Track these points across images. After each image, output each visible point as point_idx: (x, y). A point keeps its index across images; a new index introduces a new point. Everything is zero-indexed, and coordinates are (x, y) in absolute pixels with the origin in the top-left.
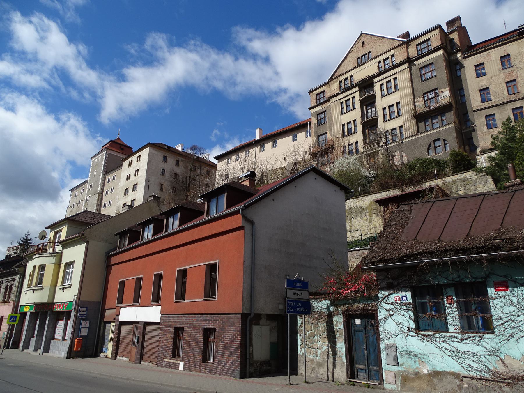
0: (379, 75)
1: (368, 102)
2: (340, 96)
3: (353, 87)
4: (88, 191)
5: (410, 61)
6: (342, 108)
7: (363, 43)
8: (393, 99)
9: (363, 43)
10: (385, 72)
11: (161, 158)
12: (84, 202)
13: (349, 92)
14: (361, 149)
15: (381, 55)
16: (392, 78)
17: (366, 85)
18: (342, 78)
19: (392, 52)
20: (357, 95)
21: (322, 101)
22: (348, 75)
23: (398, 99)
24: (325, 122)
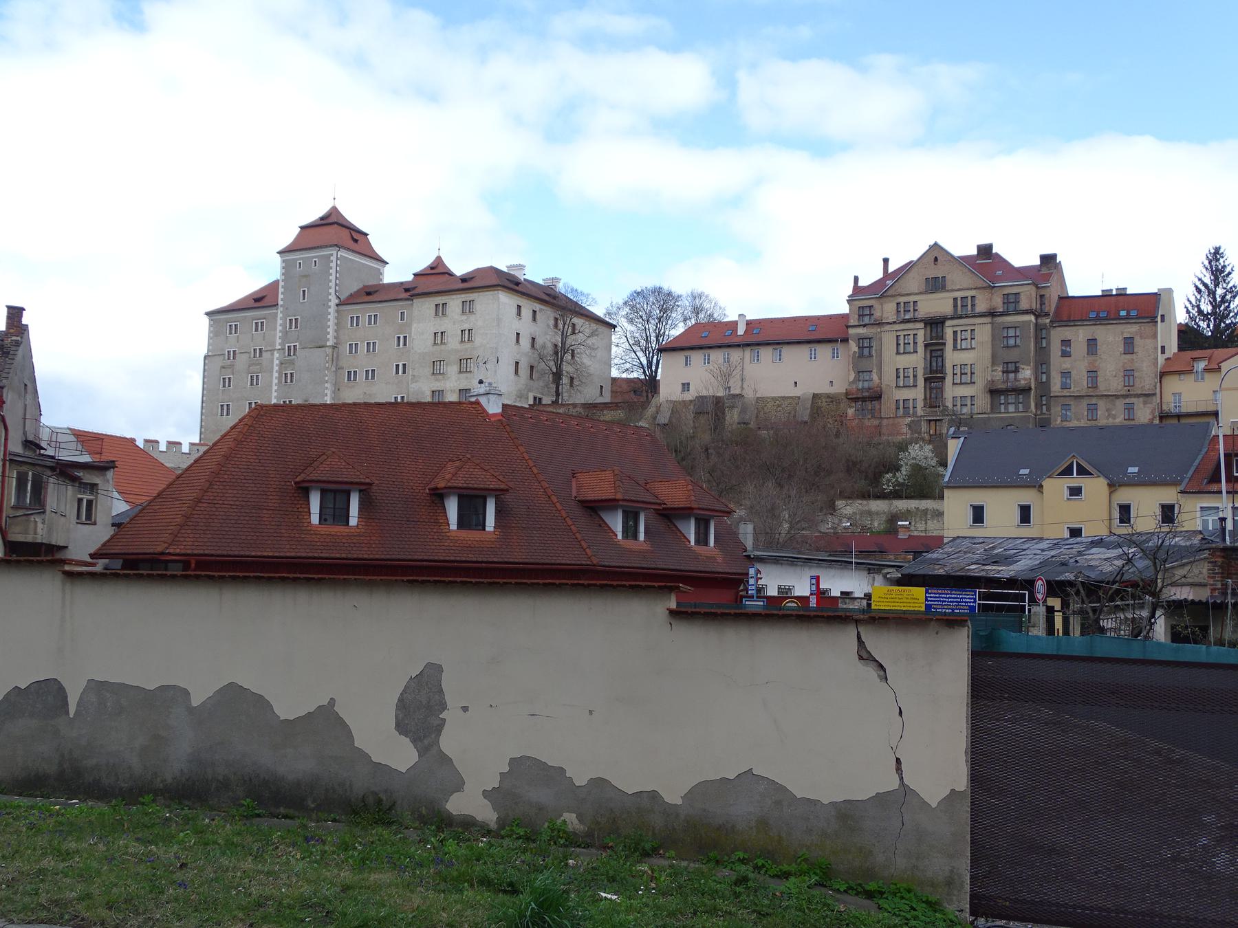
0: (952, 318)
1: (935, 350)
2: (897, 327)
3: (914, 320)
5: (992, 314)
6: (898, 344)
7: (936, 259)
8: (966, 357)
9: (936, 259)
10: (961, 317)
11: (515, 310)
12: (276, 355)
13: (911, 326)
14: (920, 412)
15: (959, 290)
16: (969, 328)
17: (935, 324)
18: (902, 300)
19: (973, 293)
20: (921, 333)
21: (867, 320)
22: (911, 299)
23: (972, 356)
24: (870, 355)
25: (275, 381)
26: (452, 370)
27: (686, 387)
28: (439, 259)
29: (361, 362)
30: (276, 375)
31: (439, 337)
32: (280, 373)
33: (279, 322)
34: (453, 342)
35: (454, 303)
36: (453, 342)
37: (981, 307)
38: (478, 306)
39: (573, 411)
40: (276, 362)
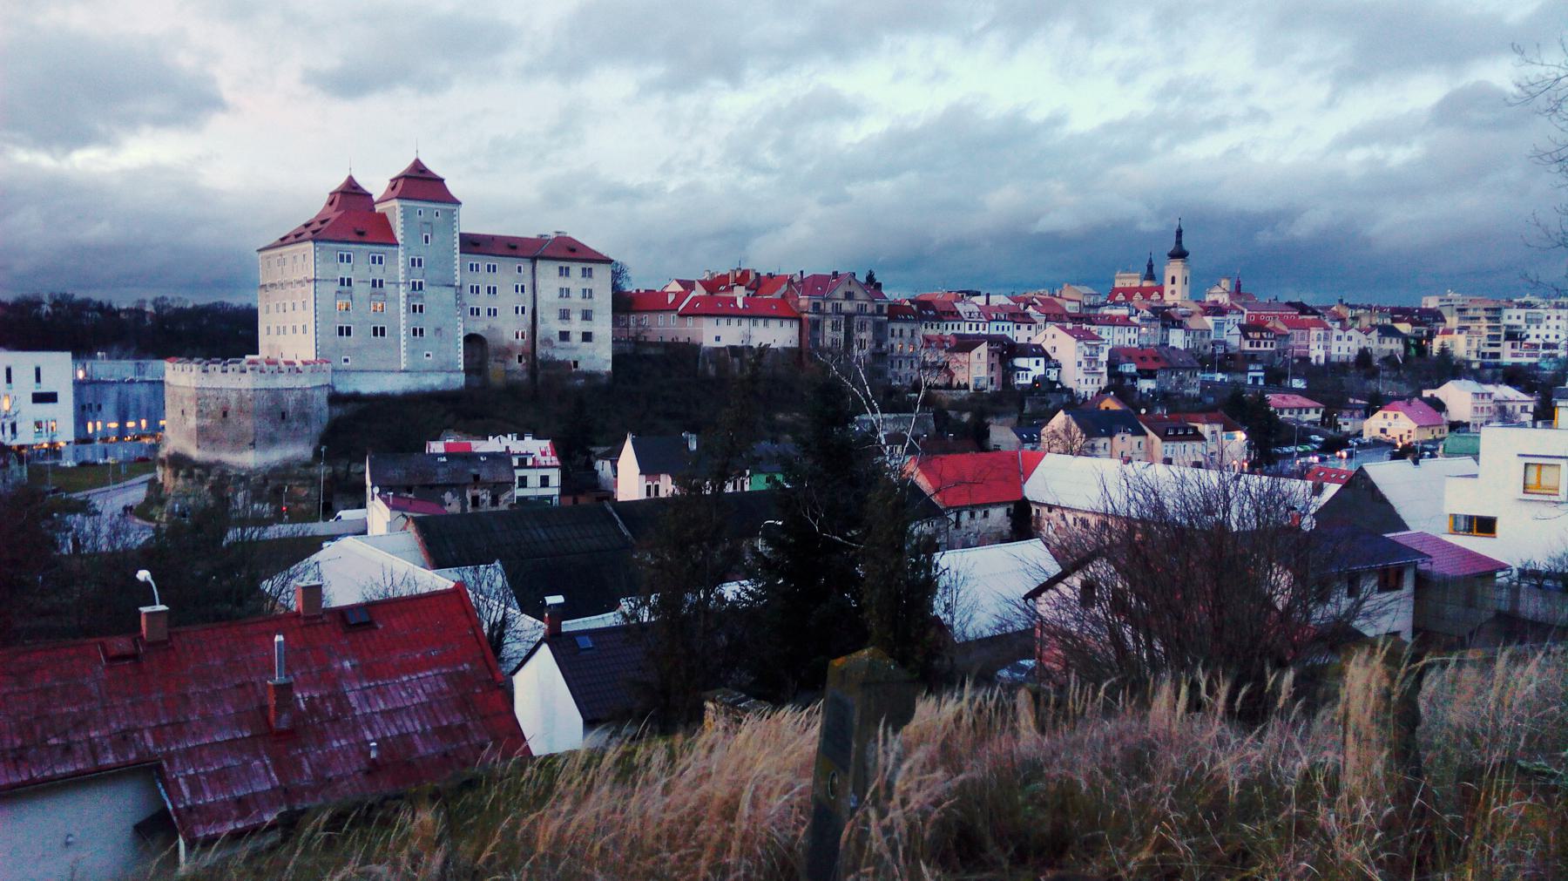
4: (408, 272)
12: (402, 288)
17: (849, 317)
25: (403, 310)
26: (576, 317)
27: (718, 339)
28: (351, 179)
29: (482, 301)
30: (403, 305)
31: (565, 293)
32: (408, 304)
33: (400, 259)
34: (576, 296)
35: (576, 269)
36: (576, 296)
37: (869, 310)
38: (594, 273)
39: (652, 351)
40: (402, 294)
